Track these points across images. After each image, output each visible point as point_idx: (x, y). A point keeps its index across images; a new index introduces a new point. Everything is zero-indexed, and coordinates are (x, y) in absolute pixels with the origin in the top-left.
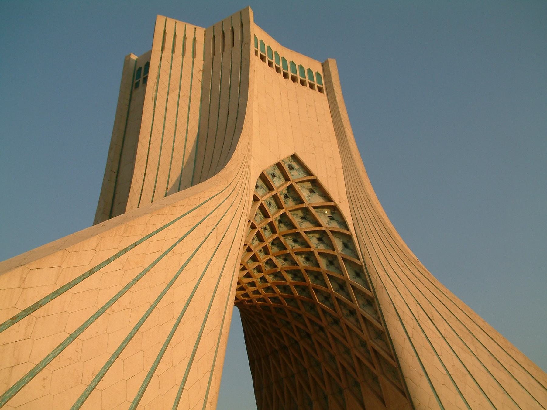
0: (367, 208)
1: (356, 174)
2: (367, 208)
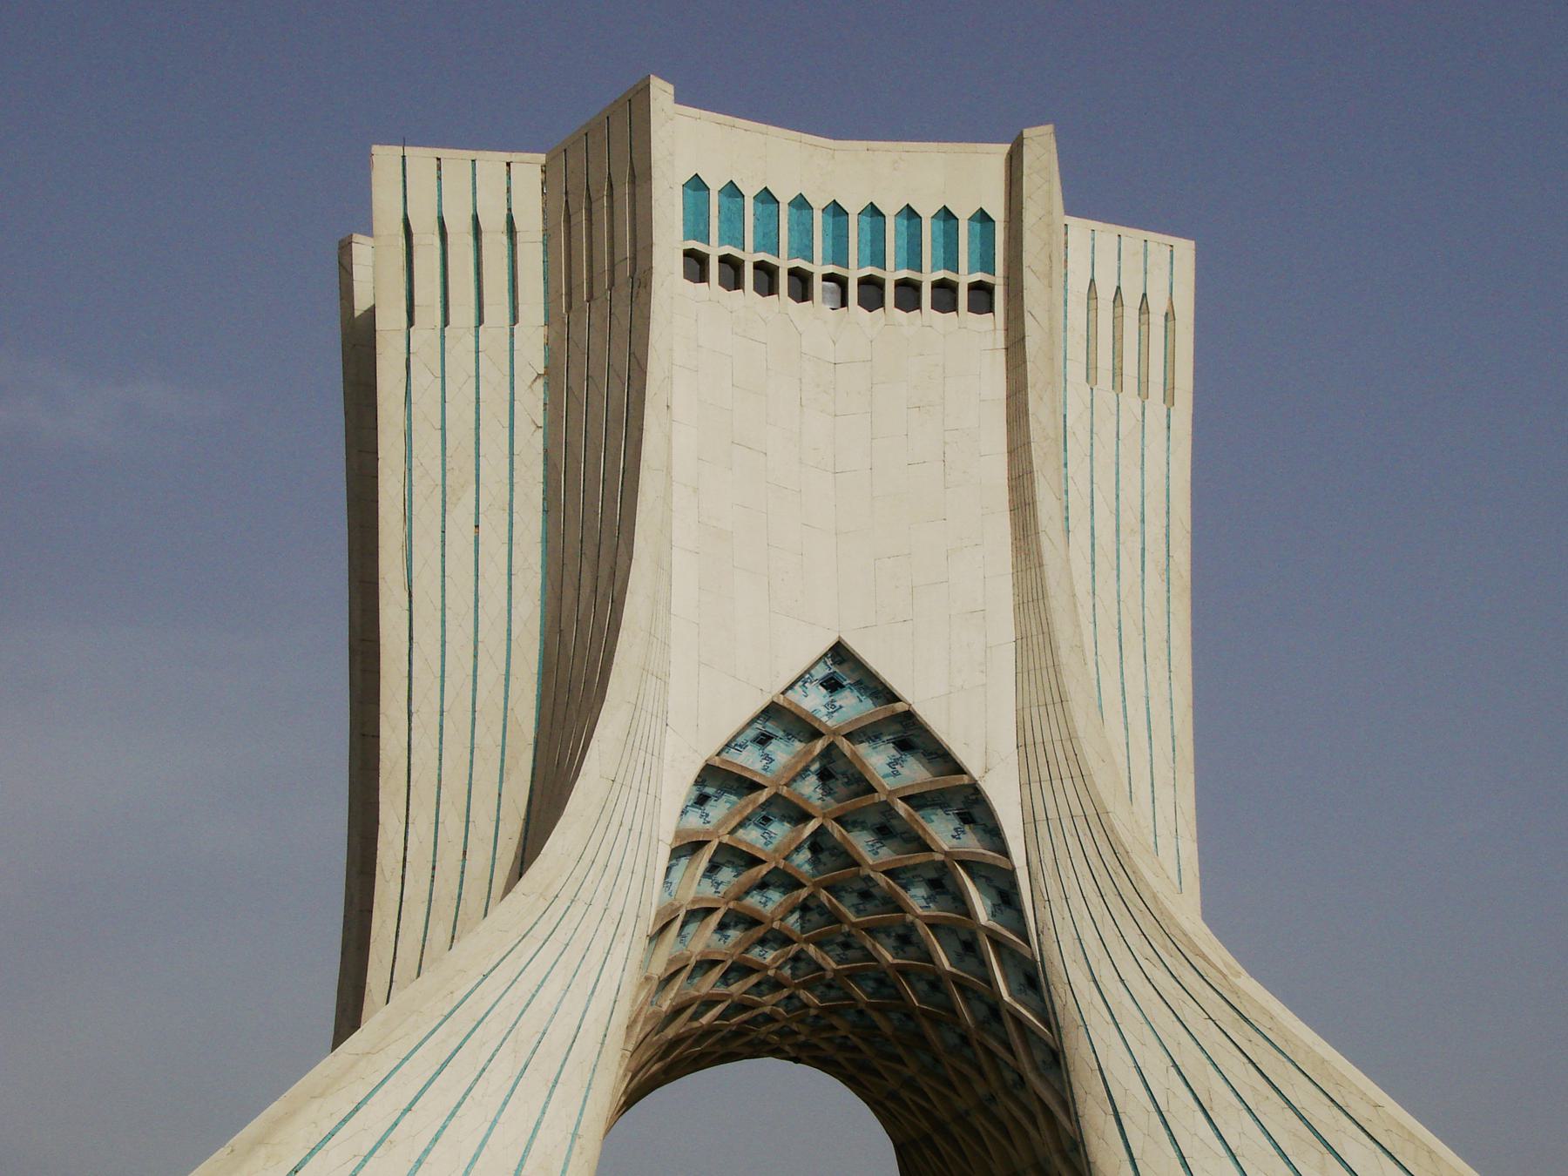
0: (1068, 783)
1: (1050, 663)
2: (1068, 783)
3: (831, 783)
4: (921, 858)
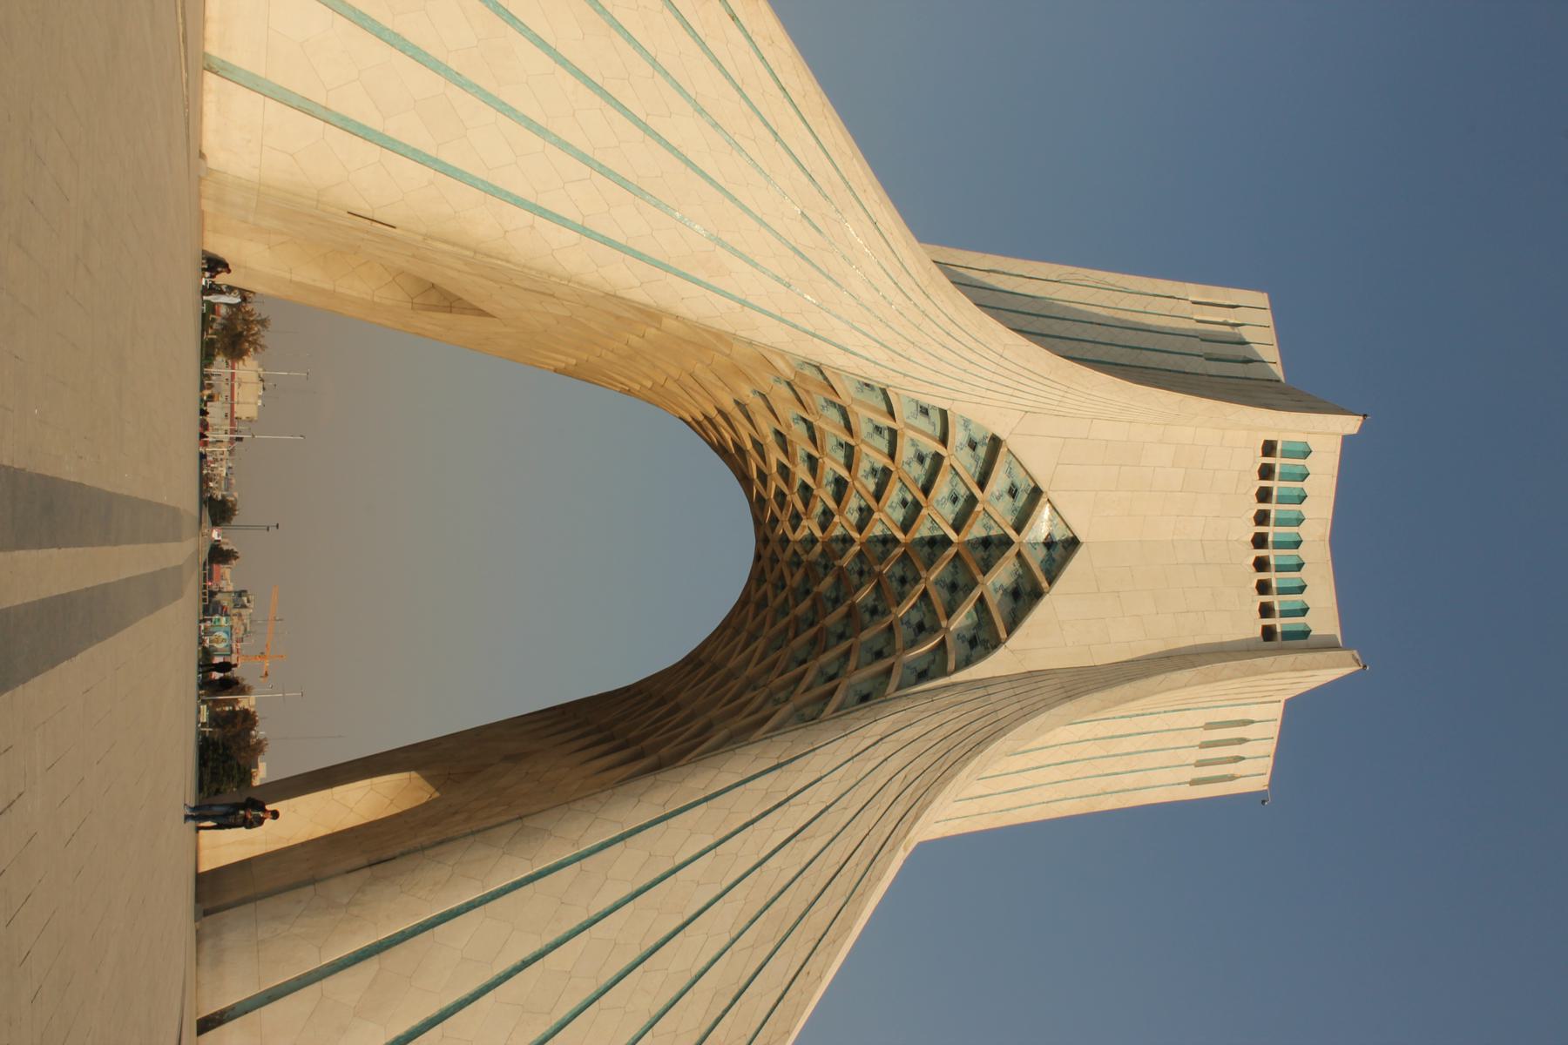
0: (1017, 706)
2: (1017, 706)
3: (981, 548)
4: (940, 611)
